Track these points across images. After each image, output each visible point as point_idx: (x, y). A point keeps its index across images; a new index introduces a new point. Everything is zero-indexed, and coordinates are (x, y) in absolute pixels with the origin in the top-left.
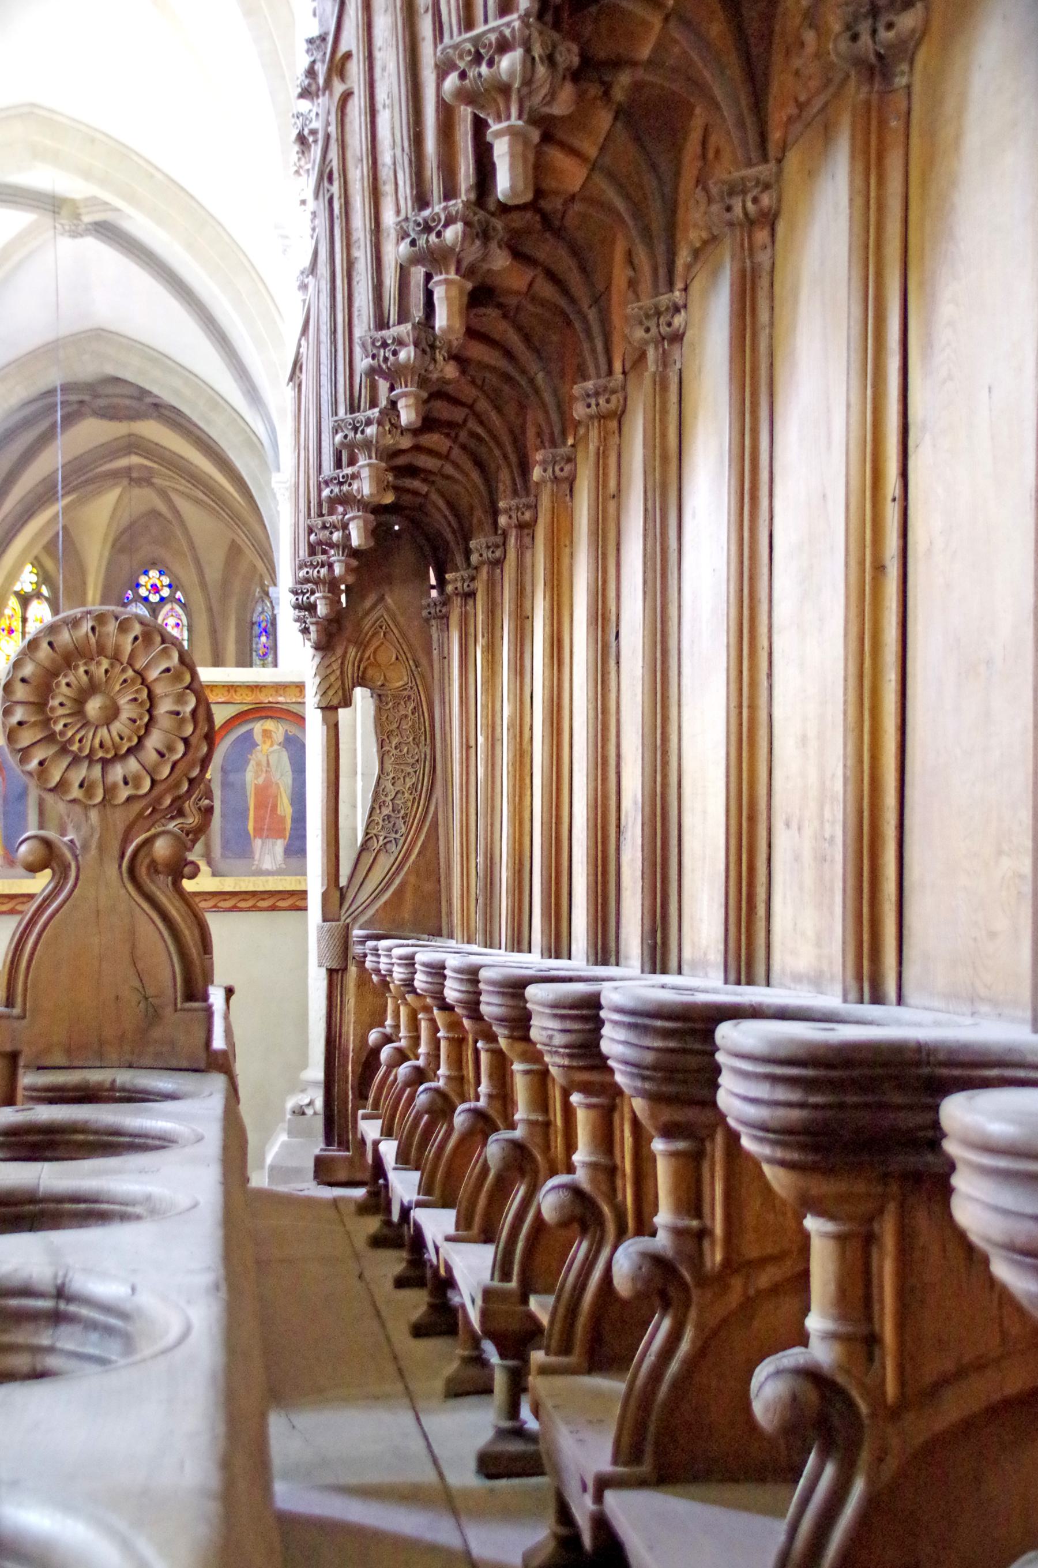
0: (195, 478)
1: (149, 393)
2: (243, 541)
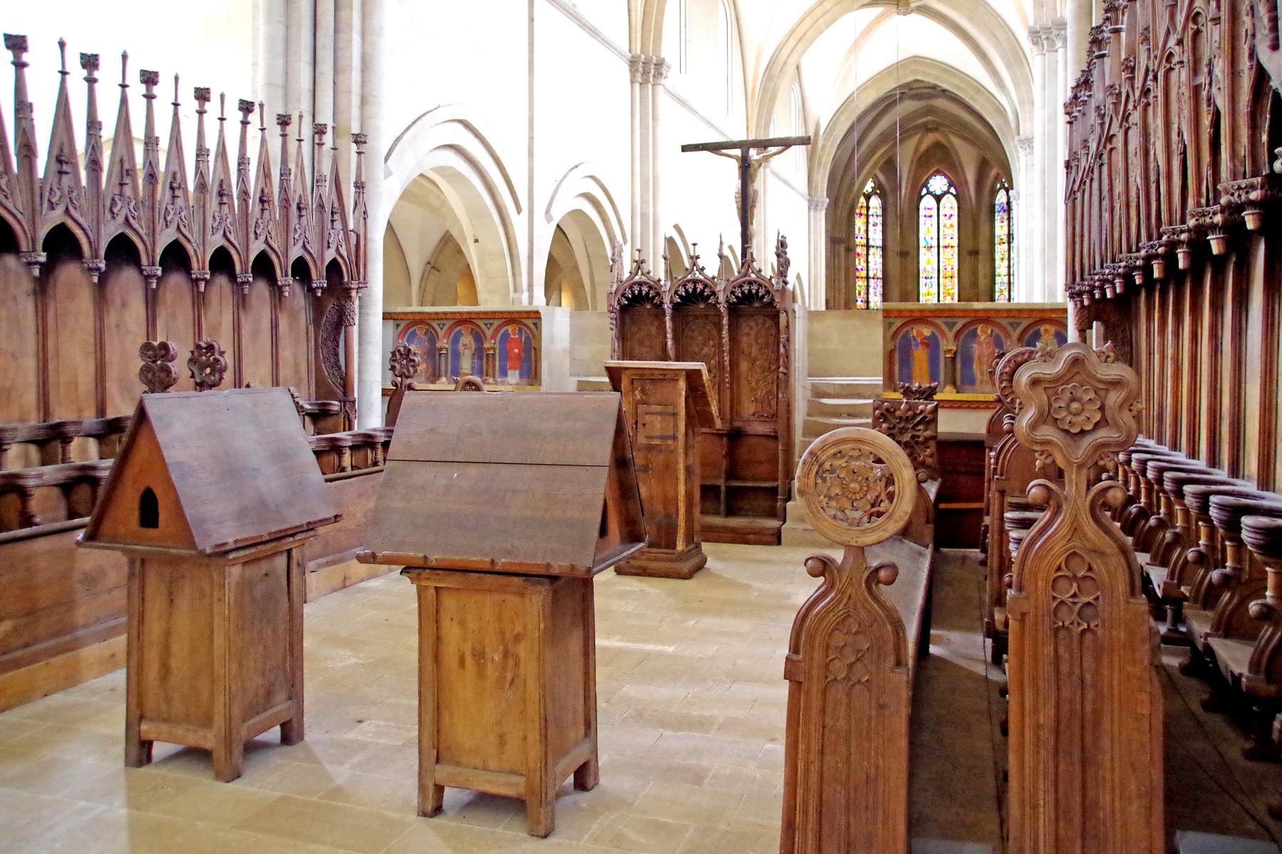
0: (964, 125)
1: (939, 86)
2: (988, 156)
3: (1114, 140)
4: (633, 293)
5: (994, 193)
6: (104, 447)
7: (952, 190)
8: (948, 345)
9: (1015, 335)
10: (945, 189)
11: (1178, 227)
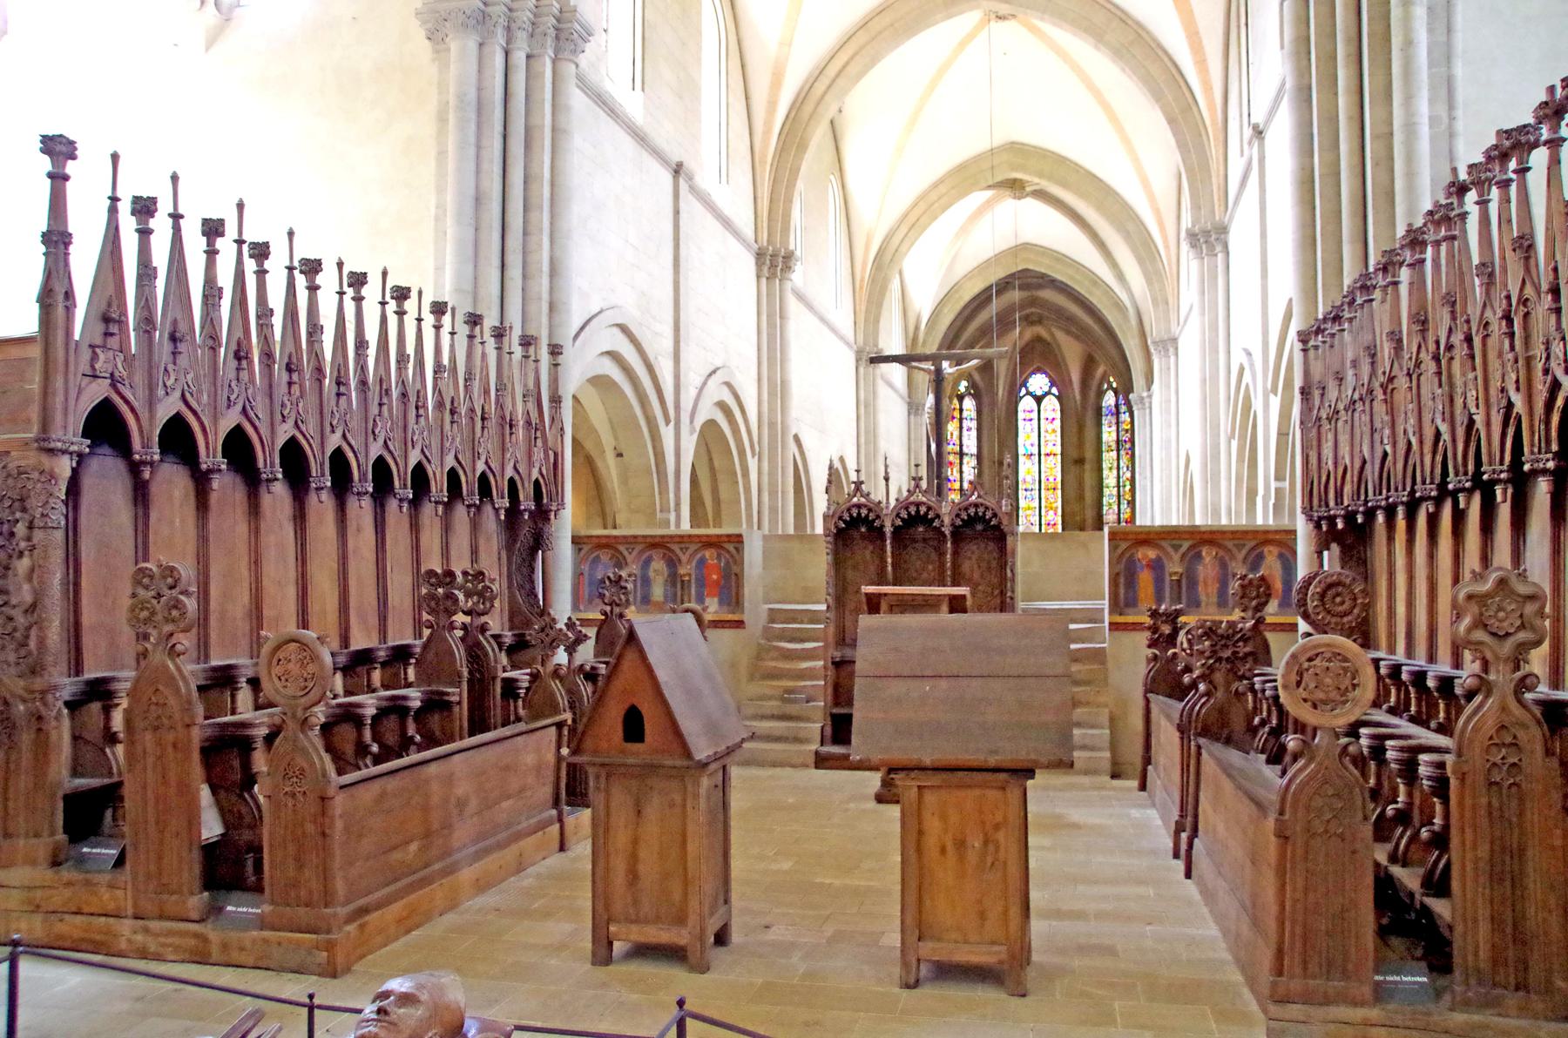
3: (1396, 381)
4: (851, 516)
5: (1100, 394)
6: (350, 681)
7: (1054, 390)
8: (1174, 567)
9: (1241, 555)
10: (1046, 389)
11: (1498, 468)
